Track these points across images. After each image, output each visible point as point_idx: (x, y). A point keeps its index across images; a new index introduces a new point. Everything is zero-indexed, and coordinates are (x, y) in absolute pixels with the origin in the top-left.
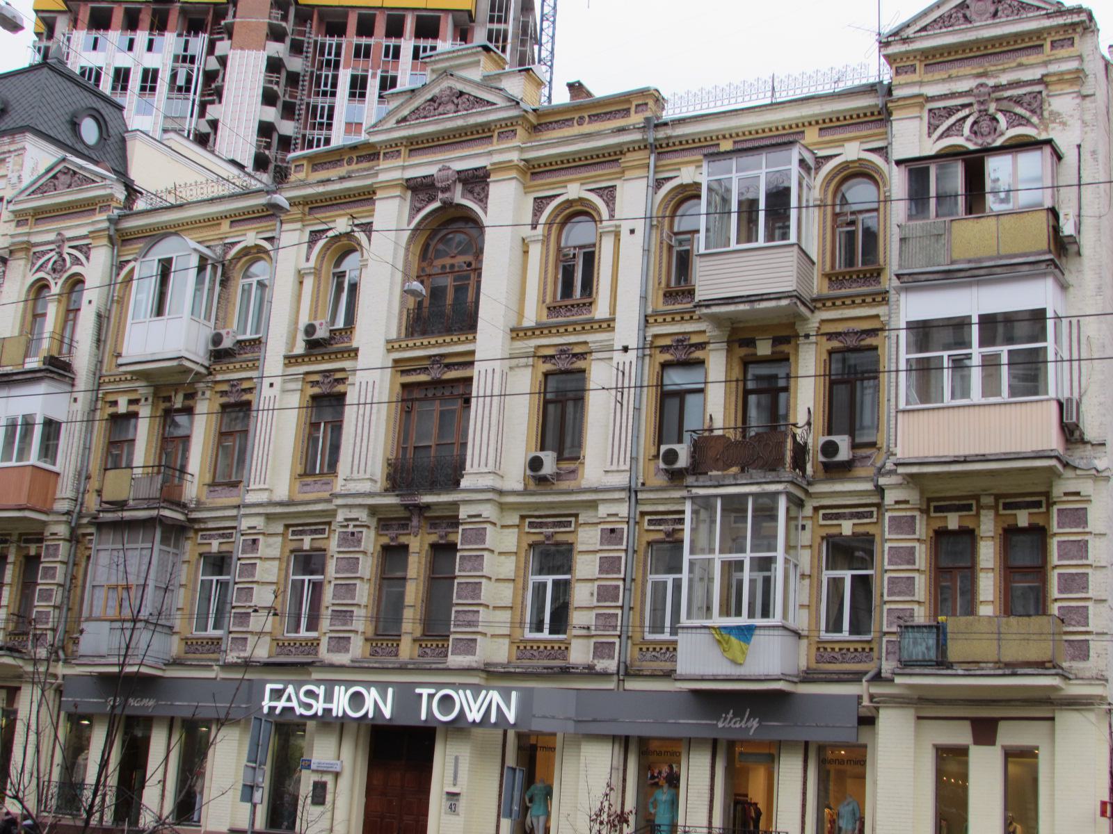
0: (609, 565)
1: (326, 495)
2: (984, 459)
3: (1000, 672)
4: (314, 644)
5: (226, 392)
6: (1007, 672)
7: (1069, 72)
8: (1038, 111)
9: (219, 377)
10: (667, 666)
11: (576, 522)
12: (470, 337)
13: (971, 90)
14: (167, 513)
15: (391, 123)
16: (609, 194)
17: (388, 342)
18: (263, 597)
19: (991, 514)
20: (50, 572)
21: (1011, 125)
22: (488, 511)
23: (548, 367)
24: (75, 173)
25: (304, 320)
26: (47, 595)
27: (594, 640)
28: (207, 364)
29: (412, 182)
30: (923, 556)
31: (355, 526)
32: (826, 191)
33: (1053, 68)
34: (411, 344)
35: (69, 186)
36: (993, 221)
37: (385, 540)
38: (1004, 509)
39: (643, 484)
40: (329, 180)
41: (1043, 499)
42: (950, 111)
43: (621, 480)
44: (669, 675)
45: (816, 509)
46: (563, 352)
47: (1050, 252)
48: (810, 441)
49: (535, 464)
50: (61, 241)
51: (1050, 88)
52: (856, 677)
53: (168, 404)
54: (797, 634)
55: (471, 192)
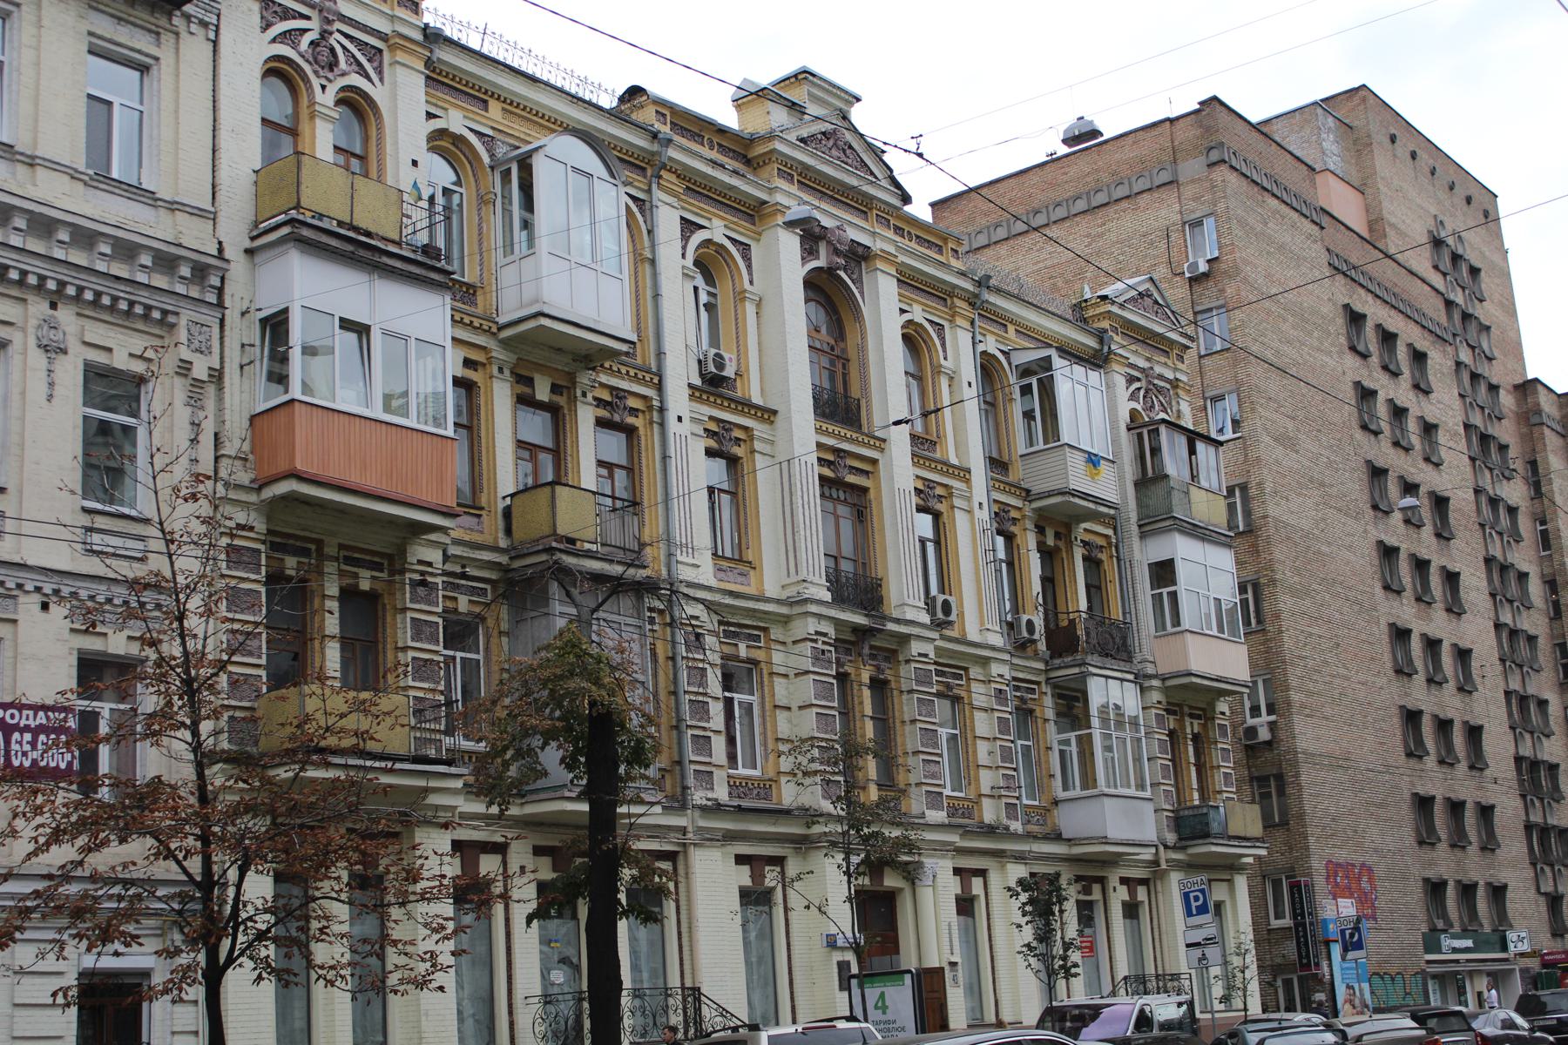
5: (637, 410)
9: (604, 378)
15: (792, 137)
27: (1004, 800)
31: (824, 643)
33: (1179, 376)
53: (527, 390)
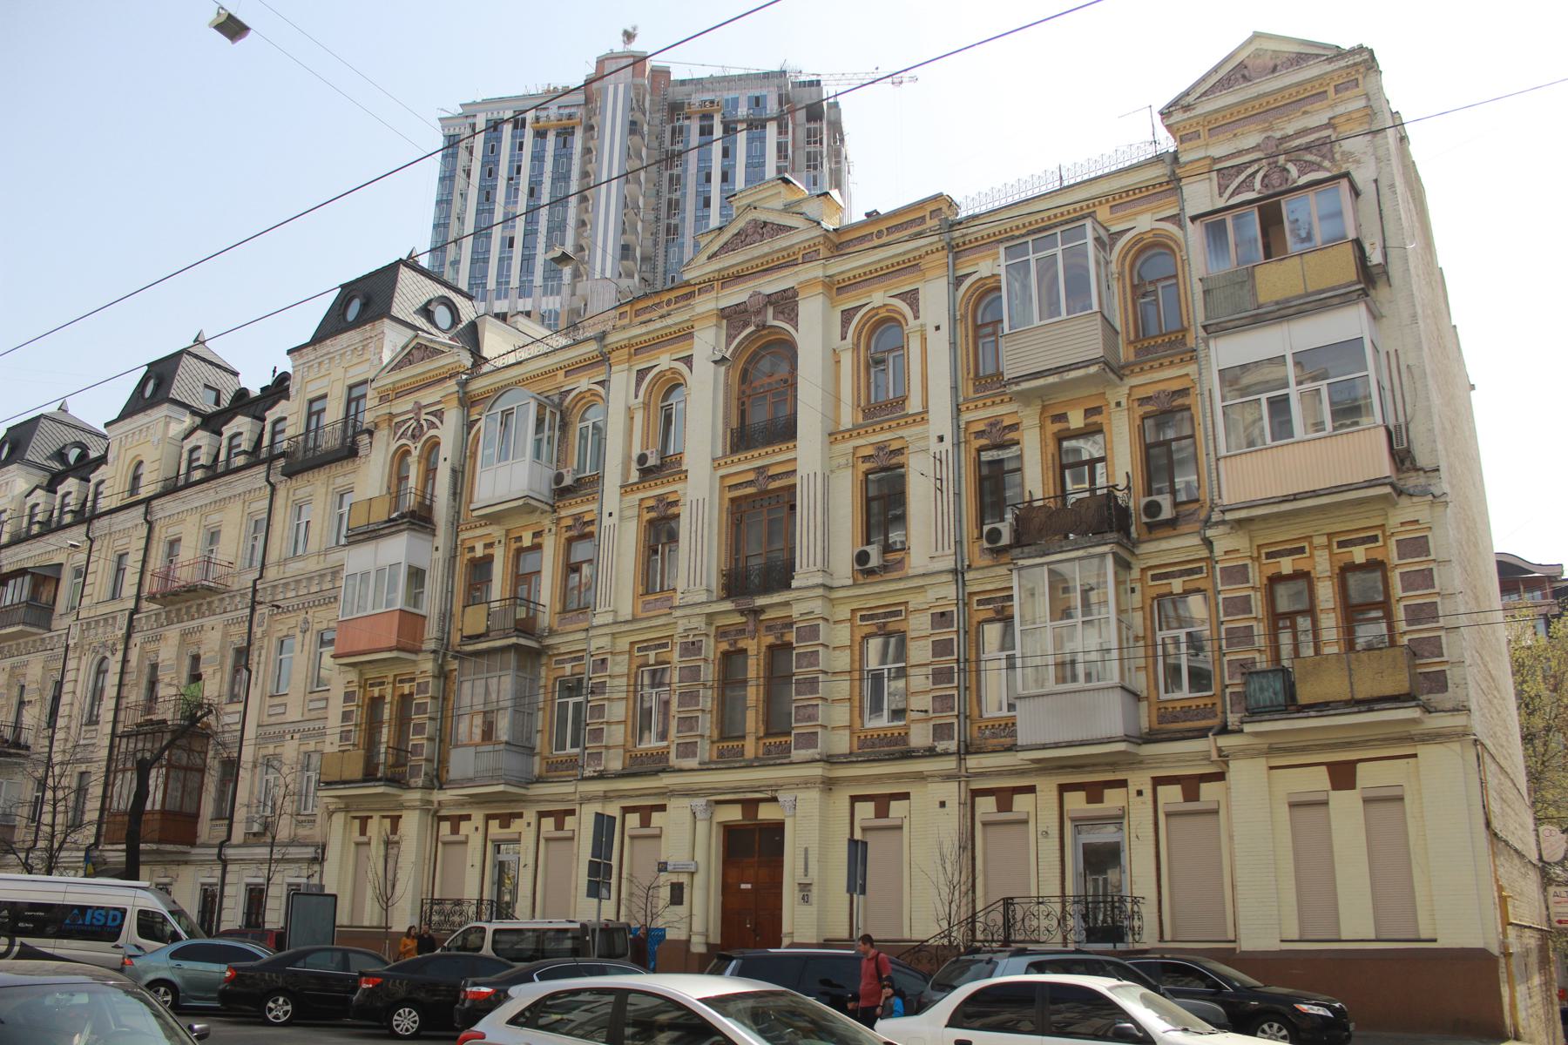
0: (941, 648)
1: (667, 611)
2: (1314, 494)
3: (1356, 709)
4: (662, 756)
6: (1363, 708)
7: (1358, 110)
8: (1329, 156)
10: (1008, 741)
11: (906, 610)
12: (791, 445)
13: (1258, 145)
14: (522, 641)
16: (911, 298)
17: (714, 460)
18: (617, 711)
19: (1326, 552)
20: (421, 708)
21: (1302, 173)
22: (817, 607)
23: (868, 465)
24: (426, 347)
25: (636, 451)
26: (420, 729)
27: (932, 723)
28: (551, 502)
29: (727, 311)
30: (1260, 603)
32: (1123, 265)
34: (735, 458)
35: (423, 359)
36: (1297, 259)
37: (724, 646)
38: (1339, 547)
39: (969, 566)
40: (650, 320)
41: (1379, 533)
42: (1240, 168)
43: (949, 563)
44: (1012, 748)
45: (1143, 570)
46: (880, 449)
47: (1359, 282)
48: (1131, 504)
49: (862, 558)
50: (419, 407)
51: (1339, 130)
52: (1202, 733)
53: (519, 544)
54: (1136, 697)
55: (782, 313)
